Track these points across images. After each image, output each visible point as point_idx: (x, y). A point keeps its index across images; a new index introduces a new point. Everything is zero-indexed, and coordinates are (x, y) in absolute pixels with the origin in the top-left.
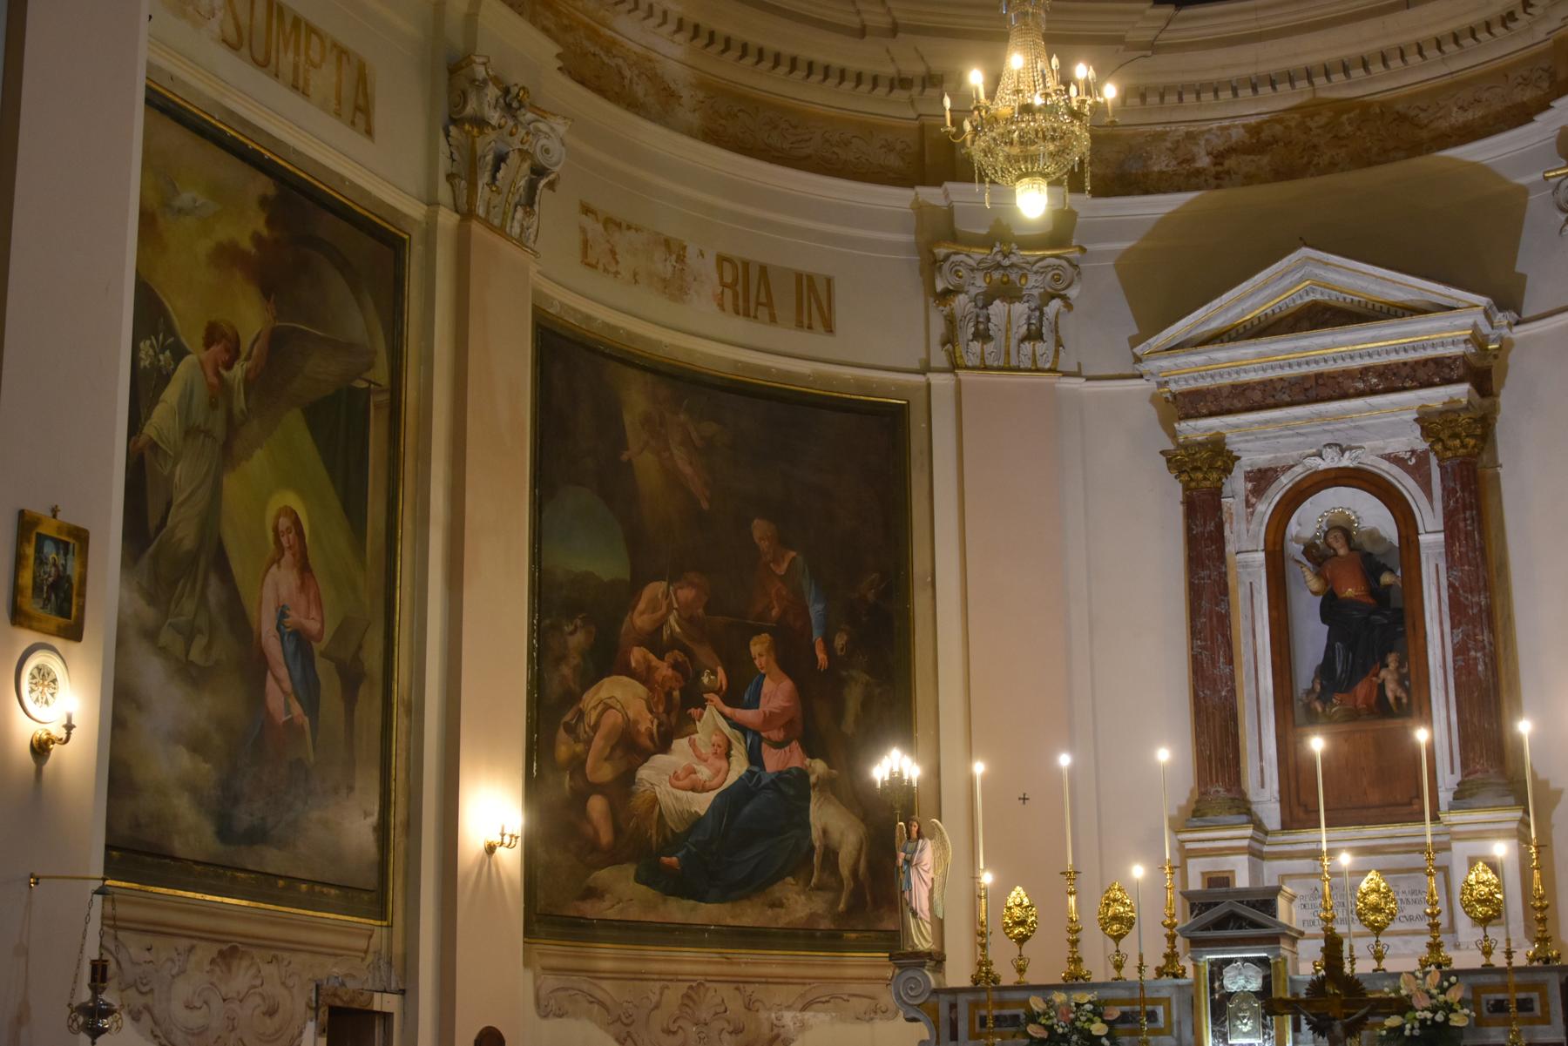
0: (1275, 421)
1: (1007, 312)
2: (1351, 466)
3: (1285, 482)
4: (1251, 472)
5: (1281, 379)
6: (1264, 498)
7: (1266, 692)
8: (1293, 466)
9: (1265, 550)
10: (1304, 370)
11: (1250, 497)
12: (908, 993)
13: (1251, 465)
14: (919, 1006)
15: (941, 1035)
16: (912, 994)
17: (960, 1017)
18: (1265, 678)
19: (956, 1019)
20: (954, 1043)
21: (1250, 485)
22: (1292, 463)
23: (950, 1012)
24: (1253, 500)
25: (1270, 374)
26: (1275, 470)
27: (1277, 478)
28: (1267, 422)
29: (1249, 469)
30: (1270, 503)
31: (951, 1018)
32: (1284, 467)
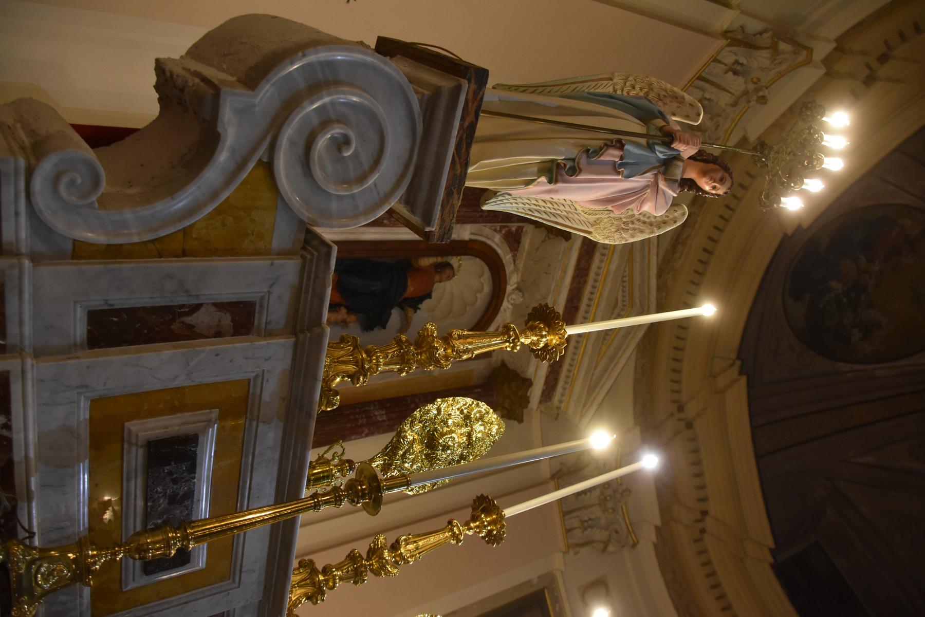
0: (563, 278)
1: (731, 90)
2: (502, 308)
3: (506, 258)
4: (522, 231)
5: (585, 282)
6: (504, 241)
7: (362, 233)
8: (514, 263)
9: (471, 241)
10: (585, 300)
11: (507, 229)
12: (325, 124)
13: (526, 231)
14: (268, 166)
15: (126, 267)
16: (322, 142)
17: (206, 349)
18: (374, 233)
19: (191, 334)
20: (79, 329)
21: (514, 229)
22: (516, 263)
23: (220, 306)
24: (503, 232)
25: (592, 276)
26: (517, 250)
27: (511, 250)
28: (565, 271)
29: (524, 230)
30: (497, 244)
31: (197, 307)
32: (516, 256)
